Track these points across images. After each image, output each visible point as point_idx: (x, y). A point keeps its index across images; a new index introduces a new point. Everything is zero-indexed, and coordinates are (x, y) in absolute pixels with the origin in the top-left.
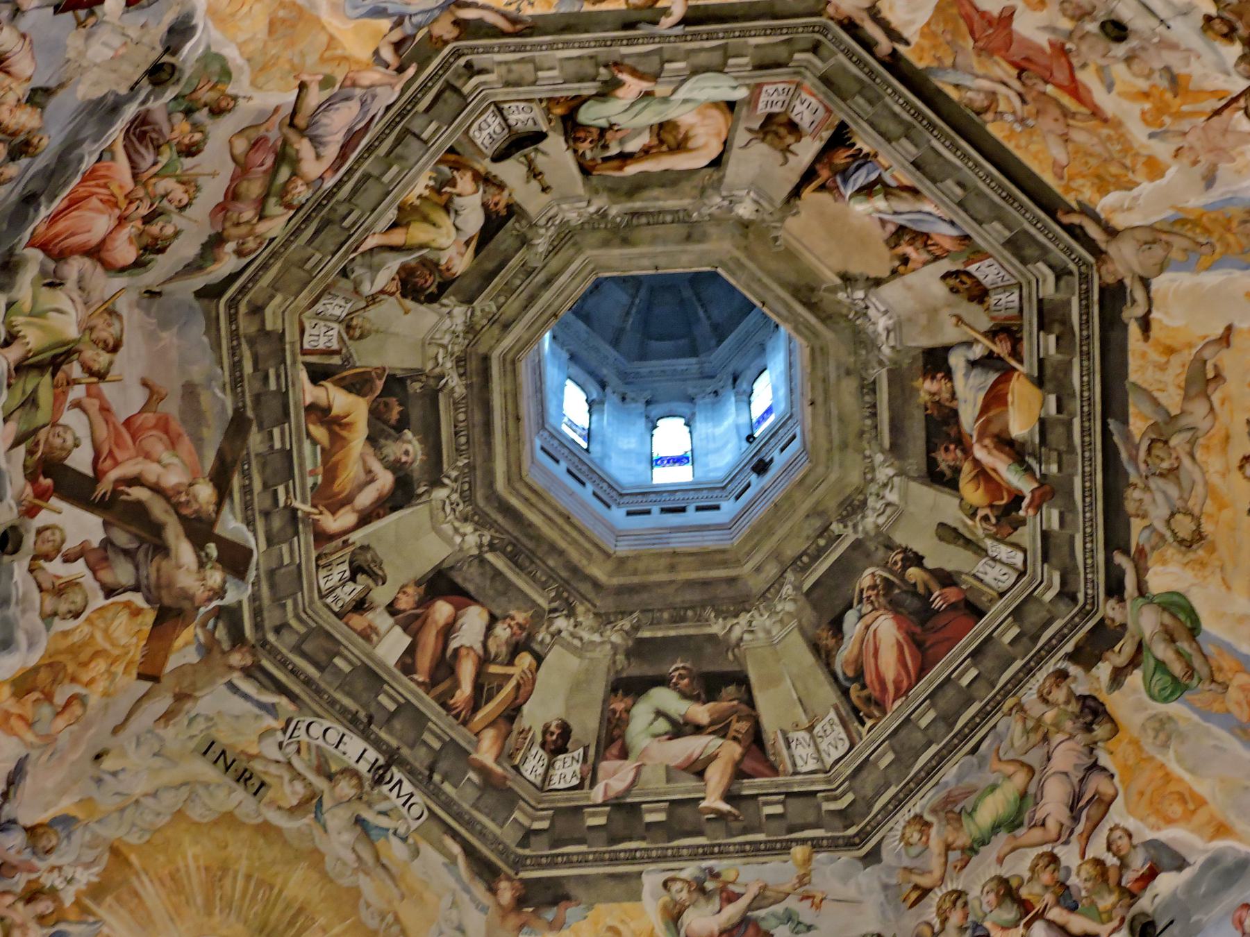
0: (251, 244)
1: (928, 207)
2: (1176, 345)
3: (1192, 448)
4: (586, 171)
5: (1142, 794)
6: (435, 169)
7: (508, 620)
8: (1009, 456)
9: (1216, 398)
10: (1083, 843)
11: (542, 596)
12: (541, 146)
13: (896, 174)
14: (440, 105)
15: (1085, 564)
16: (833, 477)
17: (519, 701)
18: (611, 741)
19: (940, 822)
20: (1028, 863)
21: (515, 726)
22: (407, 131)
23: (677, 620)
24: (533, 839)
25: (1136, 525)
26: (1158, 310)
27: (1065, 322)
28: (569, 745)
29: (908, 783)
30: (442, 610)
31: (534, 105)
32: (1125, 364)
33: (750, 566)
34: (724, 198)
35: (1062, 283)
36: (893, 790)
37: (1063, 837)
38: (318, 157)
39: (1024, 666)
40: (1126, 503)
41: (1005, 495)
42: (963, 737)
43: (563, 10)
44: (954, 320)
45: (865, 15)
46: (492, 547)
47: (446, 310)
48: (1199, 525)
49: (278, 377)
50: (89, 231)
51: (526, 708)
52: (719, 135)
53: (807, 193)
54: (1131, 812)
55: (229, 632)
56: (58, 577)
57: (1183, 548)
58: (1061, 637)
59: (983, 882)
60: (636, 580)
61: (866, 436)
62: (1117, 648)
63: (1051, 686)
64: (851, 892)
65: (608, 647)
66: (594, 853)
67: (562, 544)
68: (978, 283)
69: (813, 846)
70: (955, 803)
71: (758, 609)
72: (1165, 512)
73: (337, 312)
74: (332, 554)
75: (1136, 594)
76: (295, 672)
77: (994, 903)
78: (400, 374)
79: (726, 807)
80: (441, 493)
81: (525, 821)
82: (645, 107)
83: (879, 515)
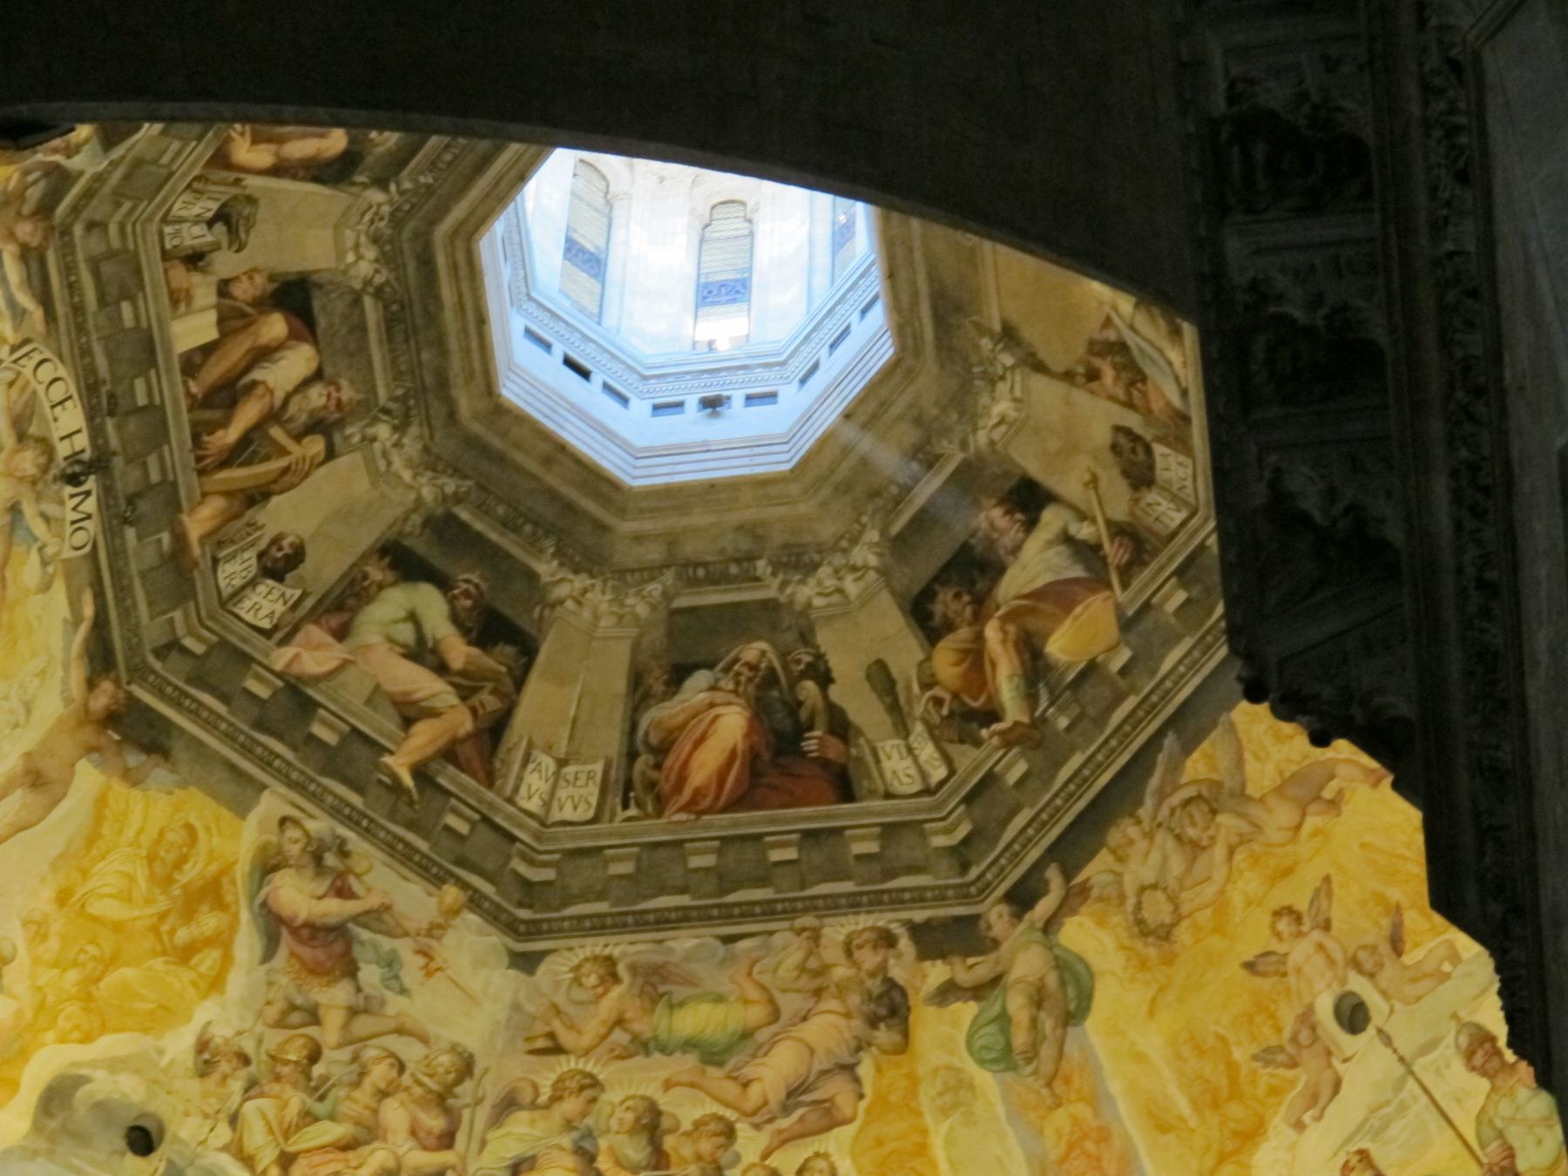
1: (1174, 355)
3: (1241, 843)
7: (332, 388)
8: (1023, 663)
9: (1311, 822)
10: (776, 1143)
11: (387, 386)
17: (275, 487)
18: (339, 607)
19: (632, 985)
20: (697, 1113)
21: (249, 515)
23: (507, 524)
24: (174, 655)
28: (289, 576)
29: (626, 913)
30: (275, 326)
33: (629, 526)
36: (602, 907)
37: (759, 1116)
39: (854, 894)
41: (983, 699)
42: (728, 914)
44: (1087, 477)
46: (378, 293)
48: (1173, 925)
51: (275, 500)
54: (854, 1156)
55: (44, 197)
57: (1136, 929)
58: (919, 897)
59: (632, 1092)
60: (497, 443)
61: (879, 502)
62: (971, 961)
63: (867, 942)
65: (413, 496)
66: (231, 724)
67: (453, 344)
68: (1151, 467)
69: (471, 900)
70: (665, 980)
71: (605, 582)
72: (1149, 876)
74: (215, 183)
75: (1040, 925)
76: (72, 288)
77: (627, 1126)
79: (408, 780)
80: (376, 196)
81: (180, 629)
83: (820, 594)
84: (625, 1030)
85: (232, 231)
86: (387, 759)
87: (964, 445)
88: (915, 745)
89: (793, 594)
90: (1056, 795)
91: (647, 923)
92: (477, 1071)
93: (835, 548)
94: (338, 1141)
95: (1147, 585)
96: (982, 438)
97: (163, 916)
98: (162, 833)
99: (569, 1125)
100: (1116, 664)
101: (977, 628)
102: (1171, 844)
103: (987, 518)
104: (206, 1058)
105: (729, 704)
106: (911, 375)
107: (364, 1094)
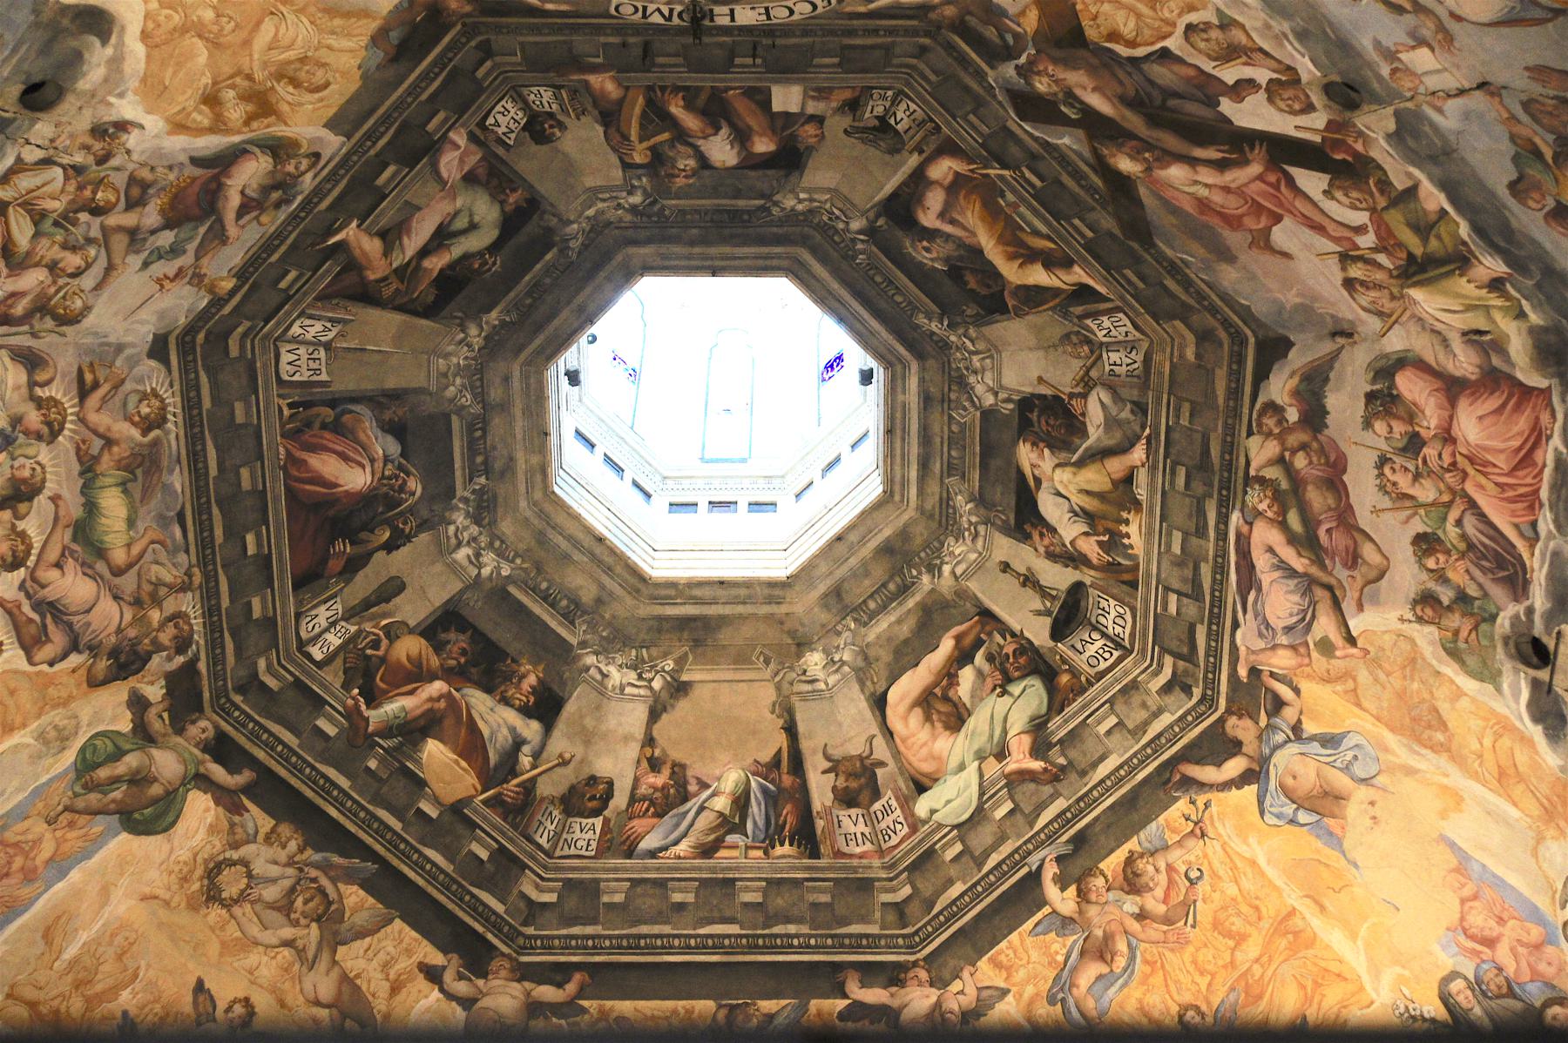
0: (1270, 422)
1: (683, 847)
3: (295, 948)
4: (986, 615)
5: (12, 693)
6: (1134, 558)
12: (1048, 621)
13: (735, 853)
14: (1184, 637)
15: (266, 730)
16: (523, 504)
19: (141, 445)
20: (32, 532)
22: (1197, 595)
25: (265, 823)
31: (1092, 672)
33: (517, 374)
34: (843, 663)
35: (522, 905)
36: (207, 403)
38: (1271, 550)
41: (382, 685)
42: (202, 510)
43: (1153, 825)
44: (567, 756)
45: (895, 1003)
46: (763, 208)
47: (1002, 396)
49: (1129, 282)
50: (1480, 418)
51: (600, 129)
52: (904, 741)
53: (781, 740)
56: (1246, 64)
57: (212, 865)
58: (216, 660)
59: (48, 469)
62: (165, 715)
64: (147, 314)
67: (697, 250)
68: (582, 815)
70: (147, 473)
72: (259, 867)
73: (1114, 357)
75: (202, 770)
76: (875, 32)
77: (17, 473)
78: (997, 316)
80: (856, 225)
82: (992, 736)
84: (102, 449)
85: (865, 130)
86: (354, 224)
87: (583, 644)
89: (458, 509)
90: (313, 768)
91: (194, 444)
92: (64, 329)
93: (494, 537)
94: (15, 245)
96: (590, 660)
97: (249, 77)
98: (324, 65)
99: (16, 421)
100: (426, 807)
102: (287, 883)
103: (528, 672)
104: (109, 132)
105: (373, 474)
106: (635, 592)
107: (55, 253)
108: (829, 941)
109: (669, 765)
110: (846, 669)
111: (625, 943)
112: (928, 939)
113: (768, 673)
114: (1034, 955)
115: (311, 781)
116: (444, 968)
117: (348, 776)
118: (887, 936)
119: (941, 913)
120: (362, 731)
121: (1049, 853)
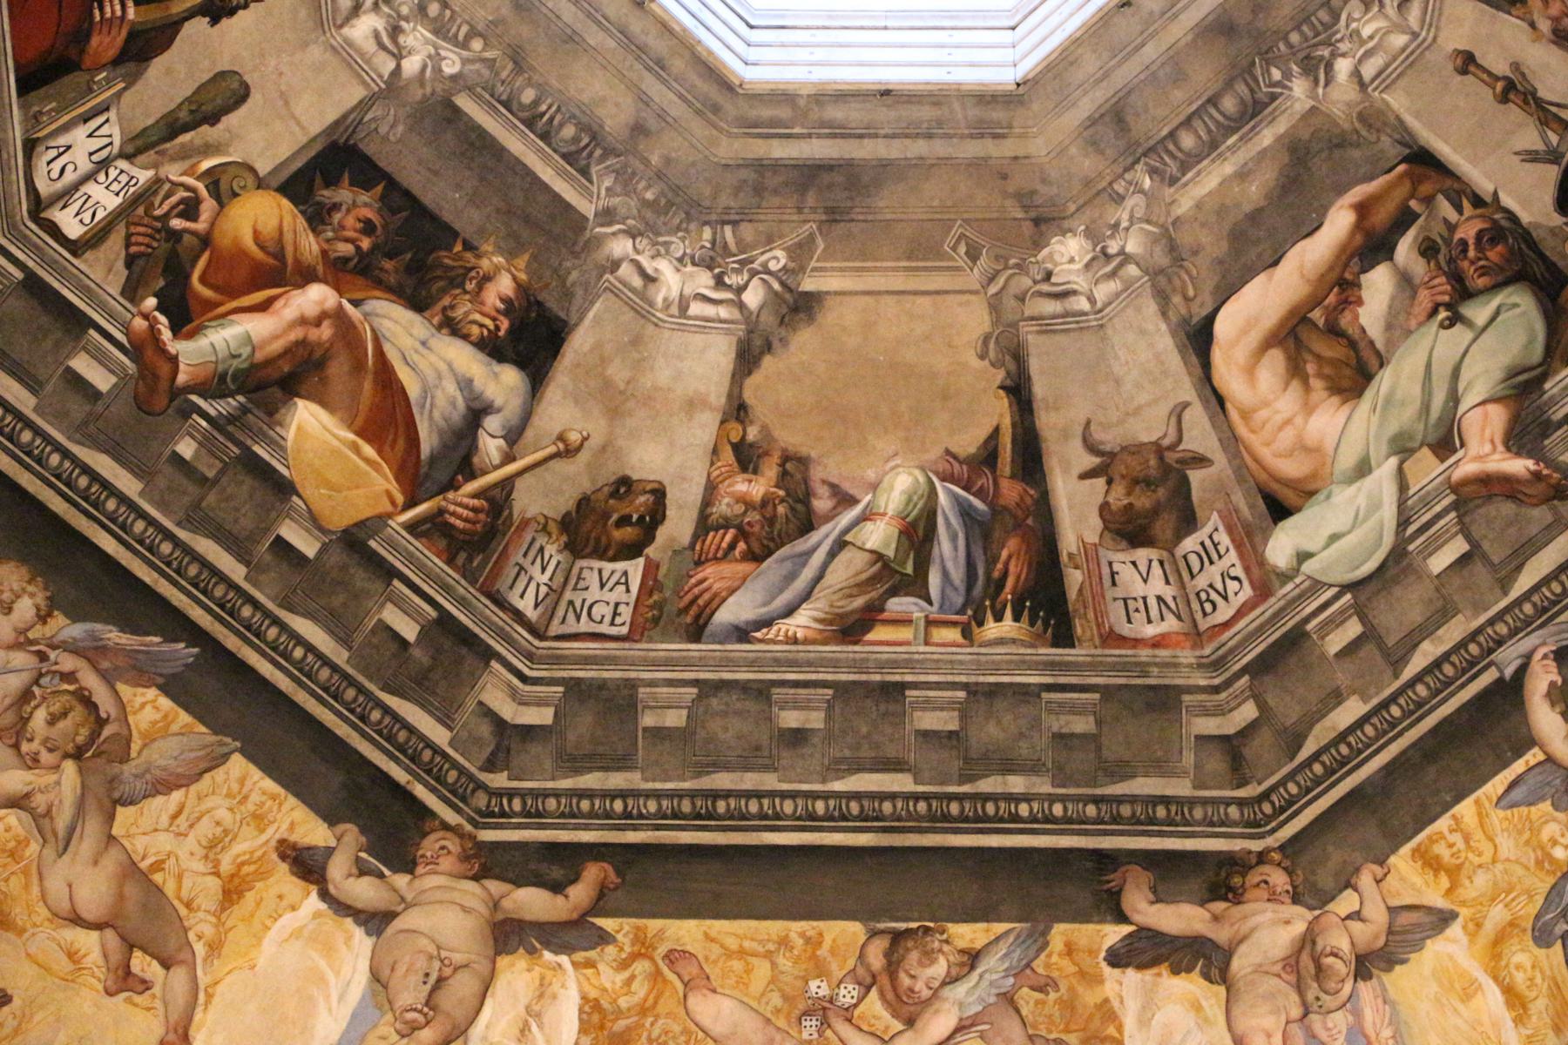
1: (801, 623)
2: (238, 911)
3: (31, 811)
4: (1423, 161)
8: (269, 362)
9: (88, 941)
13: (905, 633)
26: (317, 915)
27: (418, 687)
32: (270, 767)
34: (1126, 258)
35: (485, 730)
40: (24, 570)
41: (207, 293)
44: (574, 437)
45: (1222, 935)
52: (1246, 415)
53: (999, 411)
68: (601, 553)
82: (1426, 407)
87: (607, 216)
88: (113, 173)
90: (66, 454)
95: (421, 568)
96: (620, 247)
101: (320, 269)
103: (498, 269)
108: (1091, 810)
109: (776, 458)
110: (1132, 270)
111: (686, 806)
112: (1288, 807)
113: (974, 278)
114: (1507, 846)
115: (61, 482)
116: (330, 851)
117: (138, 471)
118: (1205, 802)
119: (1316, 757)
120: (164, 385)
121: (1540, 643)
